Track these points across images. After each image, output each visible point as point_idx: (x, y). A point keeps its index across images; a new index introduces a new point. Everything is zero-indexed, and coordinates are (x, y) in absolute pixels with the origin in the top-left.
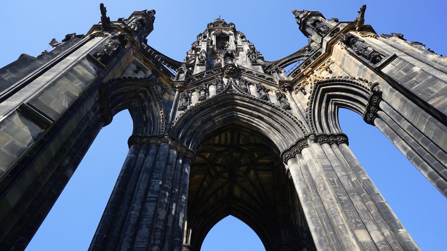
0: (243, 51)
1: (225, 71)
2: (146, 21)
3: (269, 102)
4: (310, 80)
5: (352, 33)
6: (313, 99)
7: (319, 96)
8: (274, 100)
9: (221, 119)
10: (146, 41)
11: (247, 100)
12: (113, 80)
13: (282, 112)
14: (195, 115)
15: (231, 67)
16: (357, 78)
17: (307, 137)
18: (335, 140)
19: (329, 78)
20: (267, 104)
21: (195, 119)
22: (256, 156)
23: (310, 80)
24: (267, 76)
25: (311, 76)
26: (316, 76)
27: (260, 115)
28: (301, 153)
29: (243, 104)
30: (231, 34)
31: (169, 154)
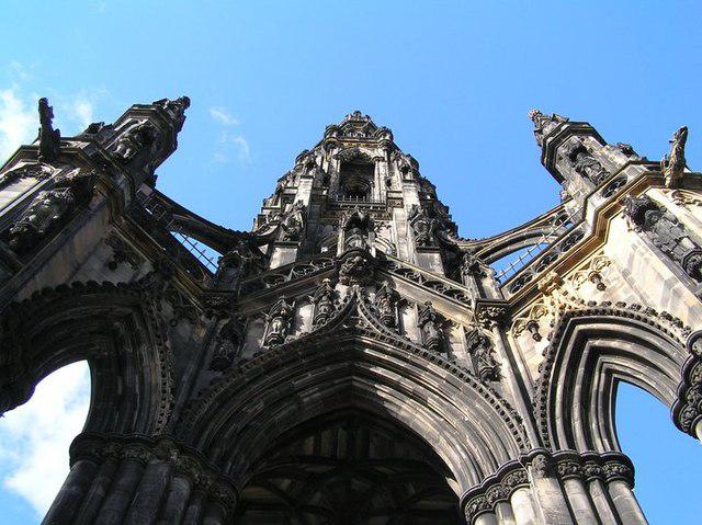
2: (159, 128)
4: (552, 304)
5: (655, 194)
6: (553, 356)
7: (569, 347)
8: (460, 351)
10: (151, 180)
11: (390, 347)
12: (46, 291)
14: (249, 383)
15: (357, 258)
16: (659, 311)
17: (527, 460)
18: (598, 470)
19: (595, 303)
22: (412, 491)
23: (552, 304)
24: (450, 284)
25: (555, 292)
26: (566, 293)
28: (509, 502)
31: (168, 490)
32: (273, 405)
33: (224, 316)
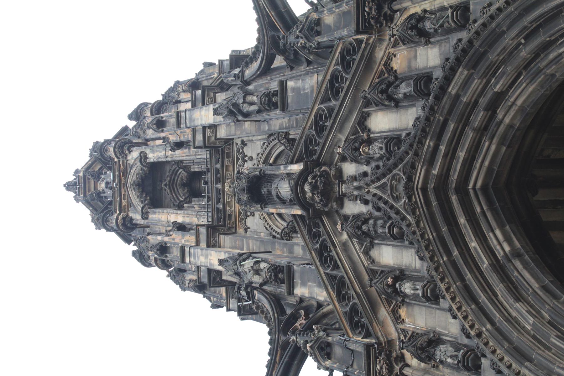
0: (214, 127)
1: (318, 206)
3: (438, 74)
8: (430, 57)
9: (498, 232)
11: (429, 143)
13: (477, 33)
14: (493, 323)
15: (307, 188)
20: (448, 79)
21: (507, 320)
27: (483, 102)
29: (445, 155)
30: (143, 157)
32: (516, 291)
33: (401, 358)
